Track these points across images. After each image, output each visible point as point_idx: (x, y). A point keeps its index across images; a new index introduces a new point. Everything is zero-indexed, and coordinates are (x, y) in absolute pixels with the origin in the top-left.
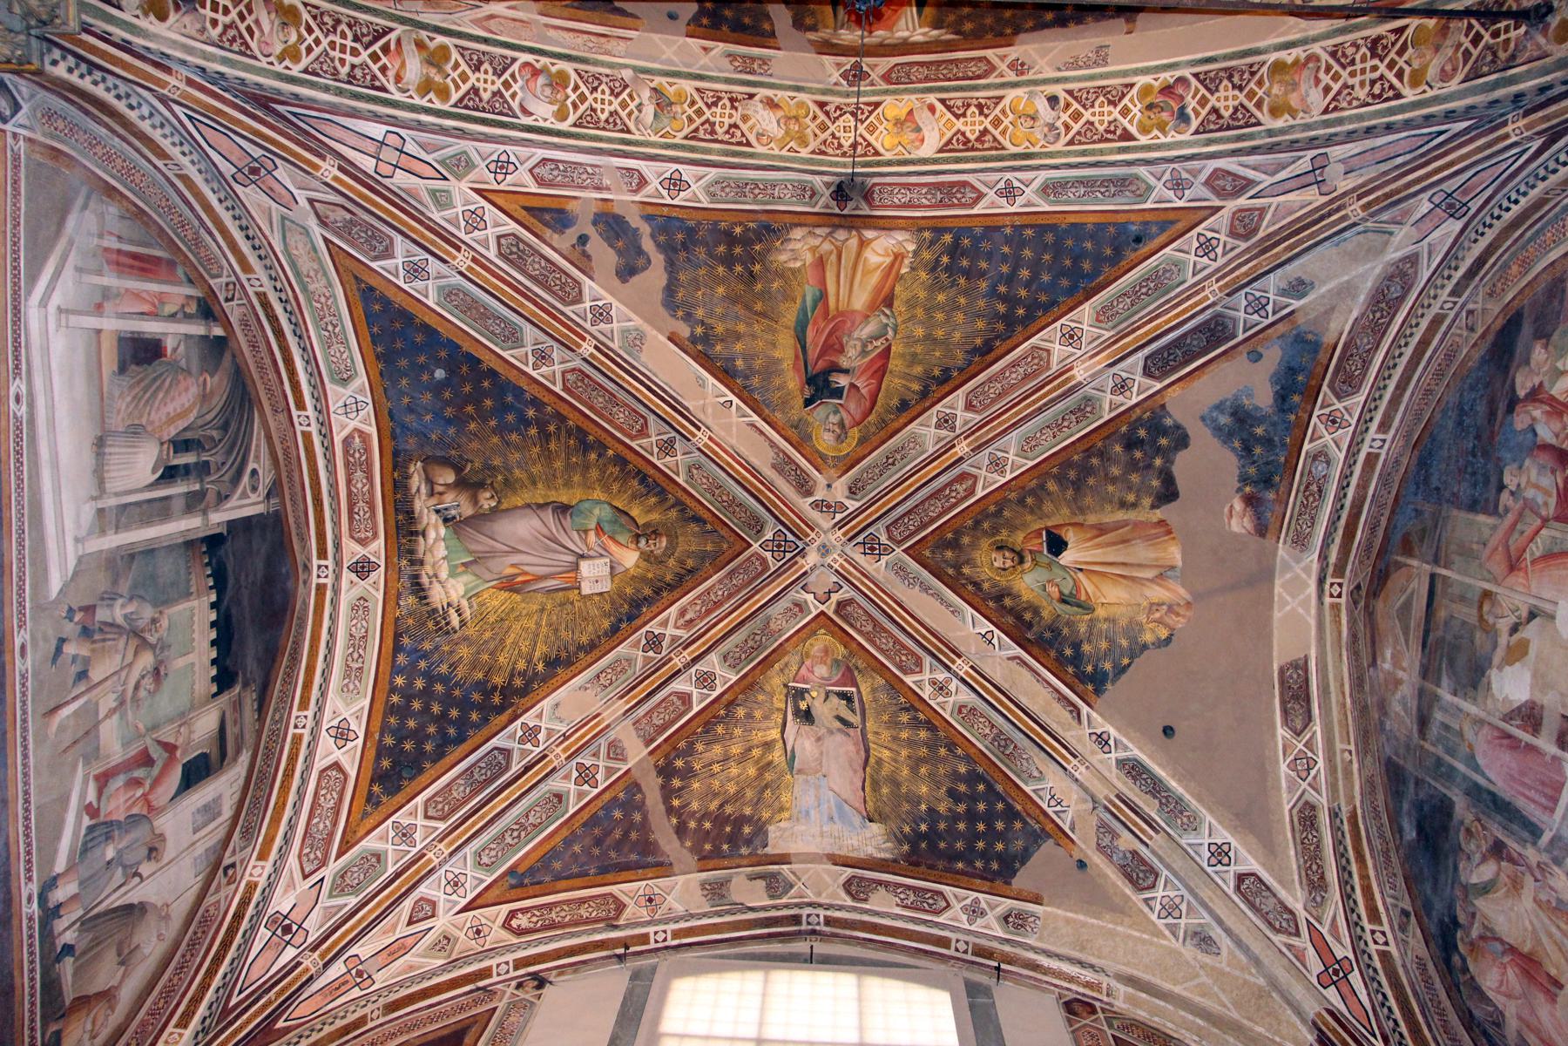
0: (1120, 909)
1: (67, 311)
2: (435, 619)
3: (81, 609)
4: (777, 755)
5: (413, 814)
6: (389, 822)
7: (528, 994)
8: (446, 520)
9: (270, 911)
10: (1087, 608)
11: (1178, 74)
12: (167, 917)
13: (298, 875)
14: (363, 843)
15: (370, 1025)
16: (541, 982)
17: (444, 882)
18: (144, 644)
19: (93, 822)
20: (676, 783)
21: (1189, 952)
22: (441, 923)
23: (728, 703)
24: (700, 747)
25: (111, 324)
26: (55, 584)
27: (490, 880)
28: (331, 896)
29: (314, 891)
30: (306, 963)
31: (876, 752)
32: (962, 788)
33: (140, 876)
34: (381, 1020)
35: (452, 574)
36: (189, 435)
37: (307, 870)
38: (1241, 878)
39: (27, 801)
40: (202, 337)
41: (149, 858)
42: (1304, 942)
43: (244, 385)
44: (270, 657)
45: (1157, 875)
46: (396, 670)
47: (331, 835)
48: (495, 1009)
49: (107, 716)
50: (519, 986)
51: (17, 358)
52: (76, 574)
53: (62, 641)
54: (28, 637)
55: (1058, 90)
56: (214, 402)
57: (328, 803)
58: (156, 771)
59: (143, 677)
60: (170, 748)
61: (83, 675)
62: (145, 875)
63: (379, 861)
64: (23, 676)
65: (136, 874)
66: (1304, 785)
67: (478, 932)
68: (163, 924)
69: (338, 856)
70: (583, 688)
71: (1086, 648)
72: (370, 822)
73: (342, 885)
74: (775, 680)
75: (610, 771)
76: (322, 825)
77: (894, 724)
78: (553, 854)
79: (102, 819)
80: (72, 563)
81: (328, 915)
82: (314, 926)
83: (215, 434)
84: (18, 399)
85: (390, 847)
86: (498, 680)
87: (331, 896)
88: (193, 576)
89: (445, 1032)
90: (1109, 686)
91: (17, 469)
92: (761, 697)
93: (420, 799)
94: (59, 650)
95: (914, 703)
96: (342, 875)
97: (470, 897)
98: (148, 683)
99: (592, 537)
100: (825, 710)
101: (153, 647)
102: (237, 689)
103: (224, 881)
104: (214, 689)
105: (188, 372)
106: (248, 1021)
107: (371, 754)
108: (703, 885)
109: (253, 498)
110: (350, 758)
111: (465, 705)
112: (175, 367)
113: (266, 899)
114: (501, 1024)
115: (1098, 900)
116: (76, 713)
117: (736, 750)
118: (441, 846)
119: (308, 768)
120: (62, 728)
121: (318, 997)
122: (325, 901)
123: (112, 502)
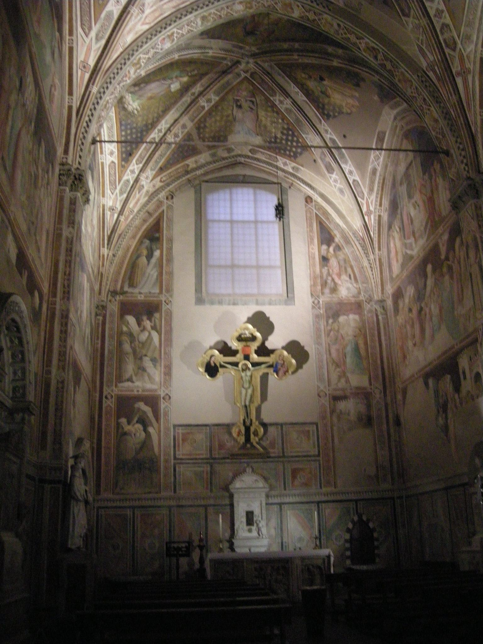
0: (323, 176)
2: (131, 114)
4: (231, 118)
7: (170, 203)
8: (131, 93)
10: (328, 96)
11: (378, 48)
16: (171, 196)
20: (202, 130)
21: (338, 193)
22: (144, 191)
23: (216, 106)
24: (208, 119)
27: (154, 172)
31: (260, 117)
32: (285, 132)
35: (134, 101)
38: (354, 181)
42: (364, 202)
45: (334, 170)
46: (122, 131)
47: (115, 180)
50: (167, 198)
55: (341, 23)
57: (112, 172)
66: (376, 163)
70: (173, 113)
71: (326, 107)
73: (121, 193)
74: (230, 97)
75: (182, 133)
77: (266, 111)
78: (170, 159)
81: (121, 201)
82: (119, 207)
86: (150, 122)
87: (120, 196)
90: (331, 119)
92: (226, 103)
93: (134, 161)
95: (273, 106)
96: (121, 190)
99: (174, 80)
100: (245, 105)
108: (210, 155)
110: (115, 159)
111: (142, 132)
115: (318, 172)
117: (218, 118)
122: (119, 198)
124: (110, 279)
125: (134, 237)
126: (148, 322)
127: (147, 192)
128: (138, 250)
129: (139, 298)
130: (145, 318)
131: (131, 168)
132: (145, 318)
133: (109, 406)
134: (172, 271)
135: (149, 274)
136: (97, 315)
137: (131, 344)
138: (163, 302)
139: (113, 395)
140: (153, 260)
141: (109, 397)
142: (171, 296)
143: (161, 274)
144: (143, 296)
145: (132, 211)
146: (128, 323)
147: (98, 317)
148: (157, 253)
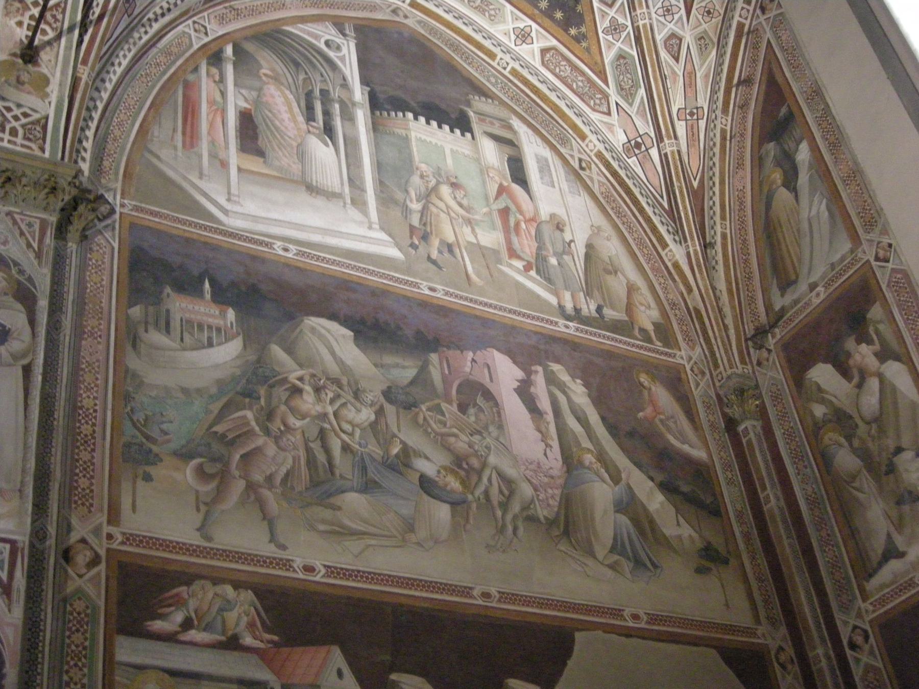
1: (229, 193)
3: (411, 237)
5: (604, 14)
6: (601, 35)
9: (620, 149)
12: (599, 229)
13: (605, 118)
14: (606, 61)
15: (728, 128)
17: (662, 19)
18: (435, 189)
19: (534, 268)
22: (688, 38)
25: (234, 157)
26: (394, 253)
28: (631, 105)
29: (622, 113)
30: (668, 150)
33: (572, 241)
34: (730, 119)
36: (303, 104)
37: (605, 110)
39: (515, 312)
40: (235, 68)
41: (562, 231)
43: (266, 34)
44: (452, 70)
47: (589, 80)
48: (769, 42)
49: (476, 237)
50: (763, 10)
51: (261, 243)
52: (390, 235)
53: (429, 258)
54: (425, 283)
56: (281, 72)
58: (513, 208)
59: (455, 198)
60: (502, 190)
61: (450, 248)
62: (571, 238)
63: (624, 58)
64: (447, 293)
65: (569, 244)
67: (709, 12)
68: (601, 233)
69: (607, 85)
72: (594, 48)
73: (628, 94)
76: (580, 83)
79: (533, 261)
80: (383, 236)
81: (641, 112)
82: (645, 127)
83: (302, 77)
84: (286, 250)
85: (619, 44)
87: (631, 105)
88: (397, 131)
89: (764, 87)
91: (327, 262)
94: (434, 262)
96: (620, 89)
97: (682, 5)
98: (460, 194)
101: (438, 183)
102: (471, 114)
103: (587, 172)
104: (468, 135)
105: (260, 90)
106: (685, 208)
107: (547, 22)
109: (345, 51)
110: (542, 39)
112: (257, 102)
113: (611, 150)
114: (782, 49)
116: (472, 262)
118: (638, 11)
119: (537, 74)
120: (478, 275)
121: (692, 150)
122: (633, 111)
123: (347, 190)
124: (727, 310)
125: (740, 165)
126: (864, 348)
127: (701, 38)
128: (761, 184)
129: (816, 301)
130: (850, 344)
131: (602, 25)
132: (850, 344)
133: (869, 668)
134: (856, 163)
135: (809, 220)
136: (731, 424)
137: (851, 445)
138: (874, 263)
139: (868, 627)
140: (803, 178)
141: (859, 640)
142: (885, 232)
143: (834, 196)
144: (820, 289)
145: (692, 113)
146: (820, 389)
147: (741, 428)
148: (803, 154)
